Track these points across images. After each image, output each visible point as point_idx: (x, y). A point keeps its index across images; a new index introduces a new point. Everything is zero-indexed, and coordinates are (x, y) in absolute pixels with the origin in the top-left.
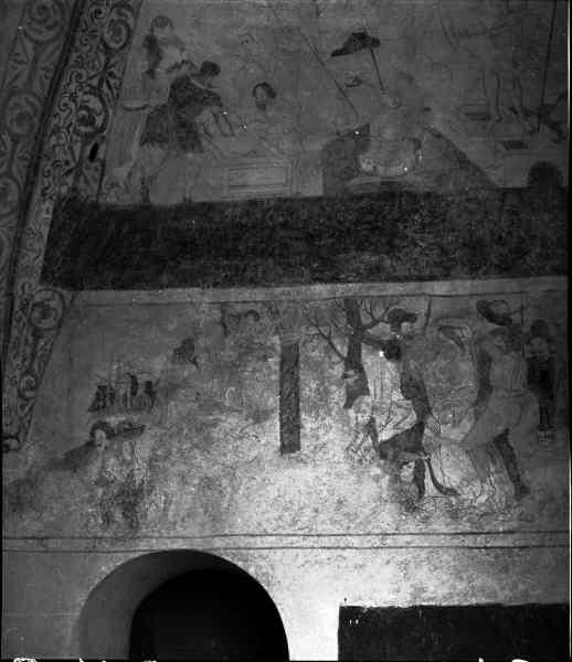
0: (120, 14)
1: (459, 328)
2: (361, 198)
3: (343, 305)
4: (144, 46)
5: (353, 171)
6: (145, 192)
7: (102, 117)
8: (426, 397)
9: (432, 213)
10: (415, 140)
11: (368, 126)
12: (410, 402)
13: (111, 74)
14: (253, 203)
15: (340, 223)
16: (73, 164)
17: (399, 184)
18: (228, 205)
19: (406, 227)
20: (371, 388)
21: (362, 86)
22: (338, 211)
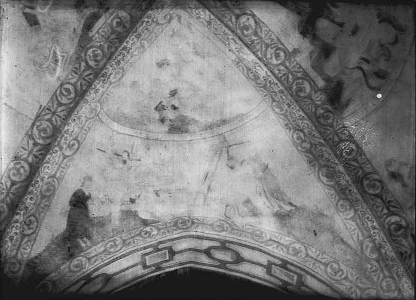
0: (368, 179)
13: (389, 202)
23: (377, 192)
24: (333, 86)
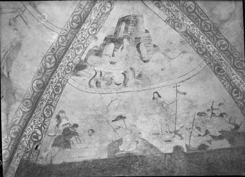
0: (49, 107)
2: (119, 158)
4: (56, 118)
7: (41, 137)
10: (136, 141)
11: (122, 138)
13: (45, 124)
14: (85, 162)
15: (112, 165)
16: (29, 150)
17: (132, 153)
18: (77, 163)
21: (120, 128)
22: (112, 162)
23: (46, 116)
24: (83, 64)
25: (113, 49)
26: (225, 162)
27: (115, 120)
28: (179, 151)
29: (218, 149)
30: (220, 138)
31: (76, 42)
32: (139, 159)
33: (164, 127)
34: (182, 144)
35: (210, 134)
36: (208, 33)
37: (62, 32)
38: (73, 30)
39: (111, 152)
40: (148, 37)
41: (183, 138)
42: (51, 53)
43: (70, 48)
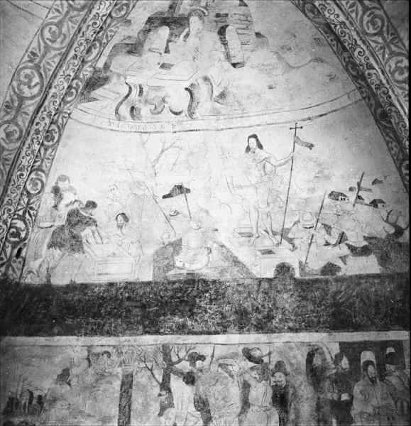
0: (37, 174)
1: (231, 365)
2: (174, 283)
3: (161, 348)
4: (52, 192)
5: (170, 267)
6: (49, 277)
7: (25, 232)
8: (209, 410)
9: (217, 292)
12: (199, 413)
13: (31, 208)
14: (111, 284)
15: (161, 297)
16: (5, 260)
19: (201, 301)
20: (175, 402)
21: (179, 216)
23: (32, 192)
24: (101, 76)
25: (167, 38)
26: (365, 303)
27: (169, 196)
28: (286, 274)
29: (356, 276)
30: (365, 251)
31: (81, 44)
32: (211, 287)
33: (262, 220)
34: (293, 260)
35: (347, 242)
36: (374, 38)
37: (51, 15)
38: (75, 13)
39: (159, 269)
40: (244, 15)
41: (296, 248)
42: (30, 64)
43: (71, 59)
